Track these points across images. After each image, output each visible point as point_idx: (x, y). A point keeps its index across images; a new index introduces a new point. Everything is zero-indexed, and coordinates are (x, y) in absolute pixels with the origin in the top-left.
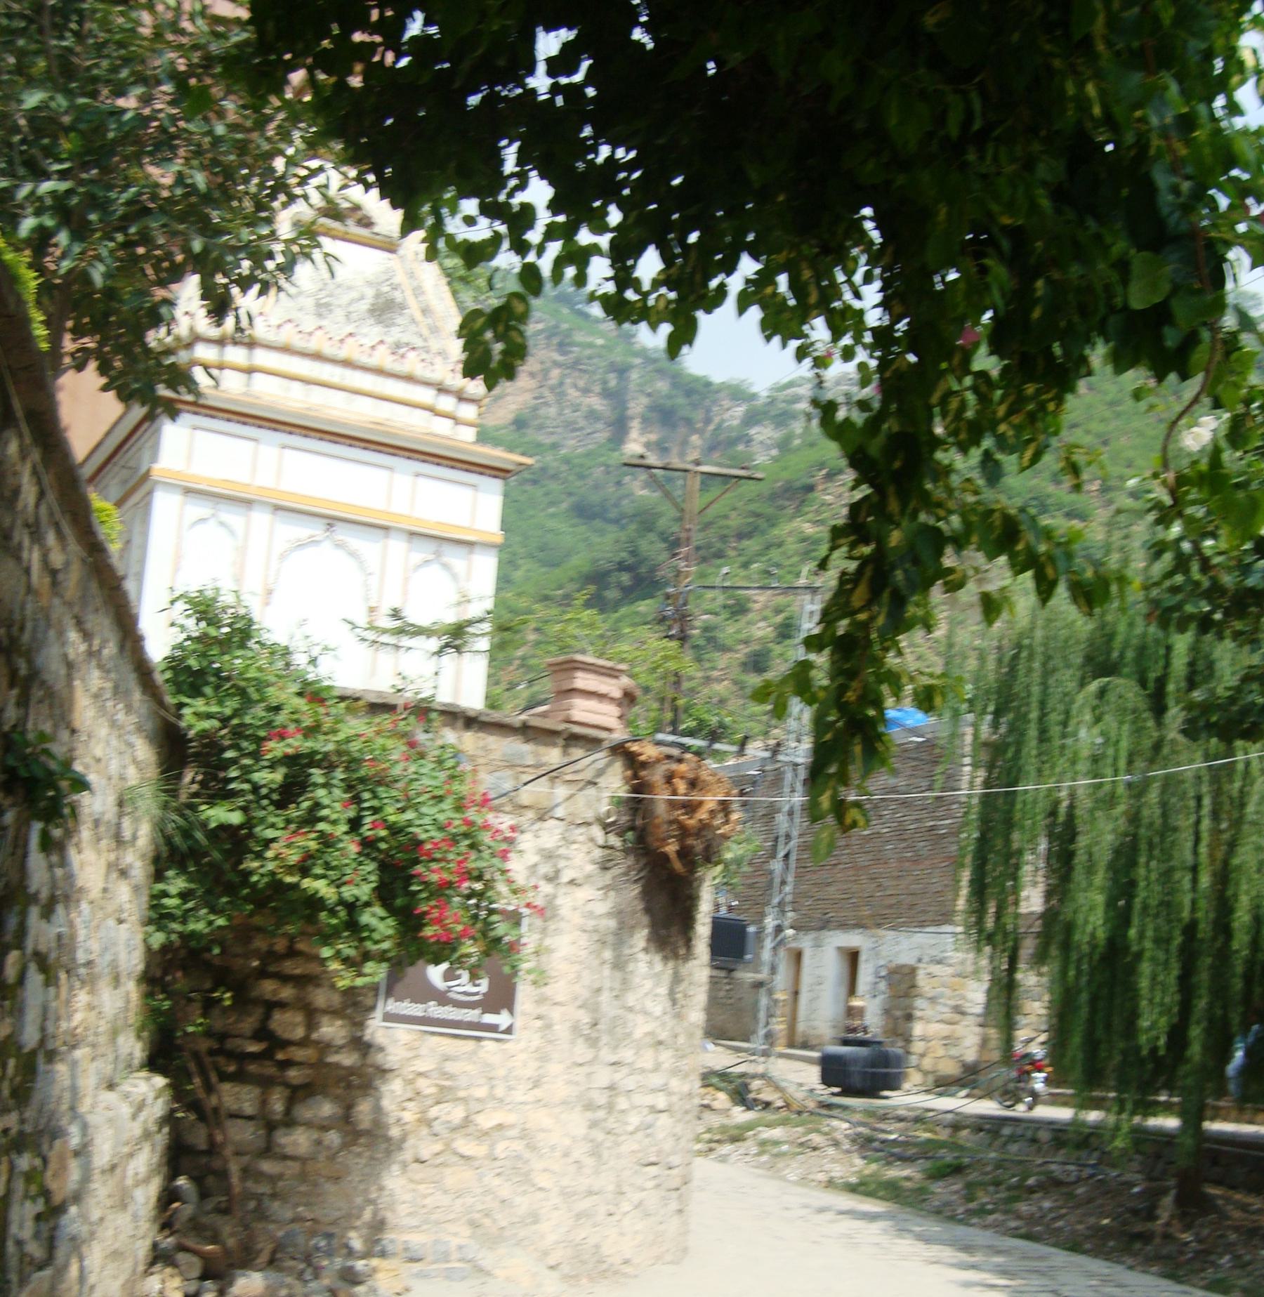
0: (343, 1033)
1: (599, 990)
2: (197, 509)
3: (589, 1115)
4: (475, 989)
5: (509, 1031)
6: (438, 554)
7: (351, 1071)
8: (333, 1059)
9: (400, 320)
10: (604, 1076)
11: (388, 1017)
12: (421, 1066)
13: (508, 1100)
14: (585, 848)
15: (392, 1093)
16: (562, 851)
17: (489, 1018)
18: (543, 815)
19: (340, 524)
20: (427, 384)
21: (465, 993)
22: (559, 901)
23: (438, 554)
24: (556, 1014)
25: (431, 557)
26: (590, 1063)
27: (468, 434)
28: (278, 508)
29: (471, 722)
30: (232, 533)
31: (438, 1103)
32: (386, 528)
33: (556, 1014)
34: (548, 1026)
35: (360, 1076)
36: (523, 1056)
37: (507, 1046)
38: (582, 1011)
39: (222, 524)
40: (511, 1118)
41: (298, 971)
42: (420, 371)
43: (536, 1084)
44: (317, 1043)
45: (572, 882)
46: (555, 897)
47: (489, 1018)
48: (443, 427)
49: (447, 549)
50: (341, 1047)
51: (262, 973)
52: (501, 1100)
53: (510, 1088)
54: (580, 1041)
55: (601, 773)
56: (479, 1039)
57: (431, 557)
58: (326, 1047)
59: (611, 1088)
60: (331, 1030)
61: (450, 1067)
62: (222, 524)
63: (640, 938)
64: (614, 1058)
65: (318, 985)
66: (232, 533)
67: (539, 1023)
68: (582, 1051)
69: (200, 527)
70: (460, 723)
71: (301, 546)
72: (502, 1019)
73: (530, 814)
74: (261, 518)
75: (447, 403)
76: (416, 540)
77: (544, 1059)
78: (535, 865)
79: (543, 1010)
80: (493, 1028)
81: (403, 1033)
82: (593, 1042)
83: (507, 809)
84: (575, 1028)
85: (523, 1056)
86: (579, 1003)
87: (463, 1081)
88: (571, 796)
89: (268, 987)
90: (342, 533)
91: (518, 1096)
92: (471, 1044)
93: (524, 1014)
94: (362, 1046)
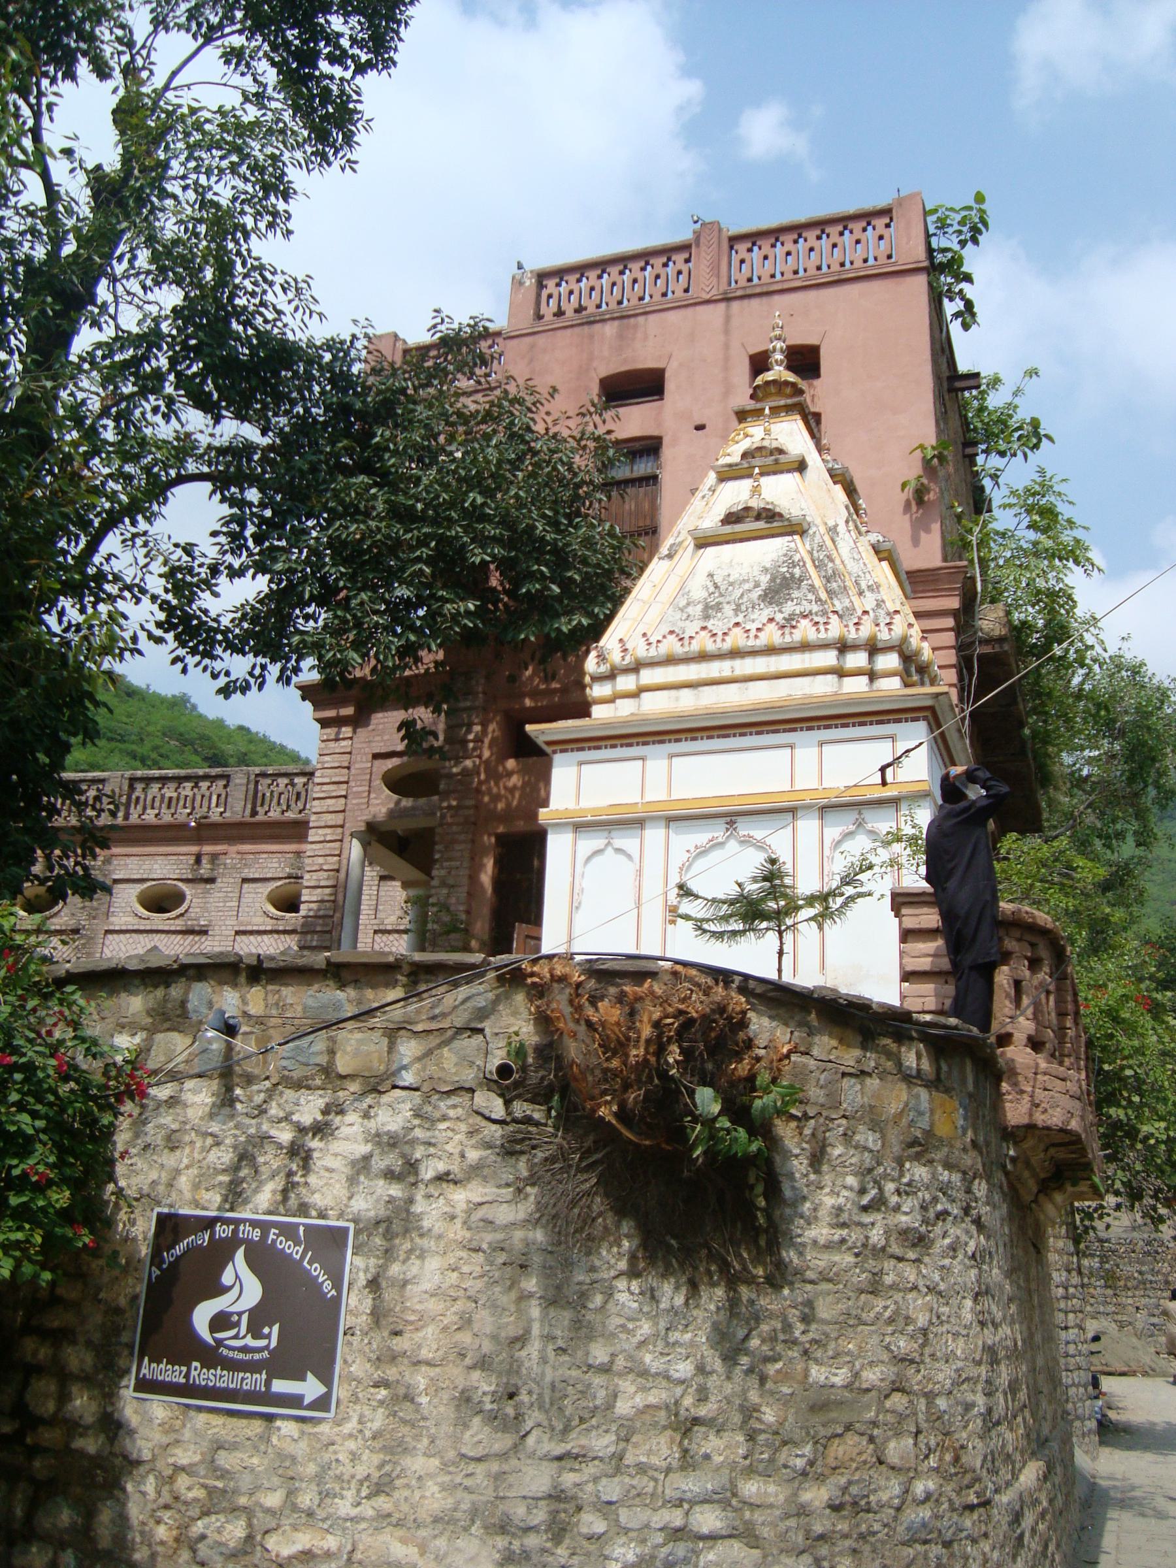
0: (94, 1407)
1: (520, 1340)
2: (589, 843)
3: (501, 1542)
4: (262, 1343)
5: (322, 1403)
6: (860, 824)
7: (97, 1461)
8: (79, 1443)
9: (795, 594)
10: (537, 1479)
11: (146, 1386)
12: (184, 1456)
13: (321, 1514)
14: (463, 1127)
15: (141, 1496)
16: (418, 1133)
17: (280, 1386)
18: (377, 1084)
19: (739, 819)
20: (824, 646)
21: (245, 1349)
22: (418, 1207)
23: (860, 824)
24: (420, 1380)
25: (852, 828)
26: (503, 1456)
27: (893, 685)
28: (670, 820)
29: (258, 972)
30: (629, 857)
31: (206, 1513)
32: (792, 811)
33: (420, 1380)
34: (409, 1398)
35: (105, 1470)
36: (352, 1445)
37: (324, 1429)
38: (476, 1375)
39: (618, 850)
40: (331, 1542)
41: (56, 1324)
42: (812, 635)
43: (381, 1487)
44: (66, 1421)
45: (443, 1178)
46: (411, 1201)
47: (280, 1386)
48: (857, 686)
49: (868, 814)
50: (87, 1428)
51: (28, 1329)
52: (310, 1514)
53: (325, 1495)
54: (477, 1421)
55: (483, 1014)
56: (270, 1418)
57: (852, 828)
58: (73, 1427)
59: (557, 1496)
60: (82, 1403)
61: (225, 1460)
62: (618, 850)
63: (613, 1258)
64: (559, 1449)
65: (74, 1342)
66: (629, 857)
67: (383, 1393)
68: (478, 1436)
69: (597, 860)
70: (242, 979)
71: (703, 852)
72: (311, 1388)
73: (354, 1087)
74: (654, 835)
75: (857, 660)
76: (830, 817)
77: (394, 1448)
78: (367, 1158)
79: (391, 1373)
80: (295, 1401)
81: (159, 1408)
82: (512, 1424)
83: (318, 1082)
84: (465, 1399)
85: (352, 1445)
86: (468, 1361)
87: (246, 1481)
88: (429, 1053)
89: (29, 1344)
90: (745, 828)
91: (344, 1507)
92: (257, 1426)
93: (351, 1378)
94: (112, 1426)
